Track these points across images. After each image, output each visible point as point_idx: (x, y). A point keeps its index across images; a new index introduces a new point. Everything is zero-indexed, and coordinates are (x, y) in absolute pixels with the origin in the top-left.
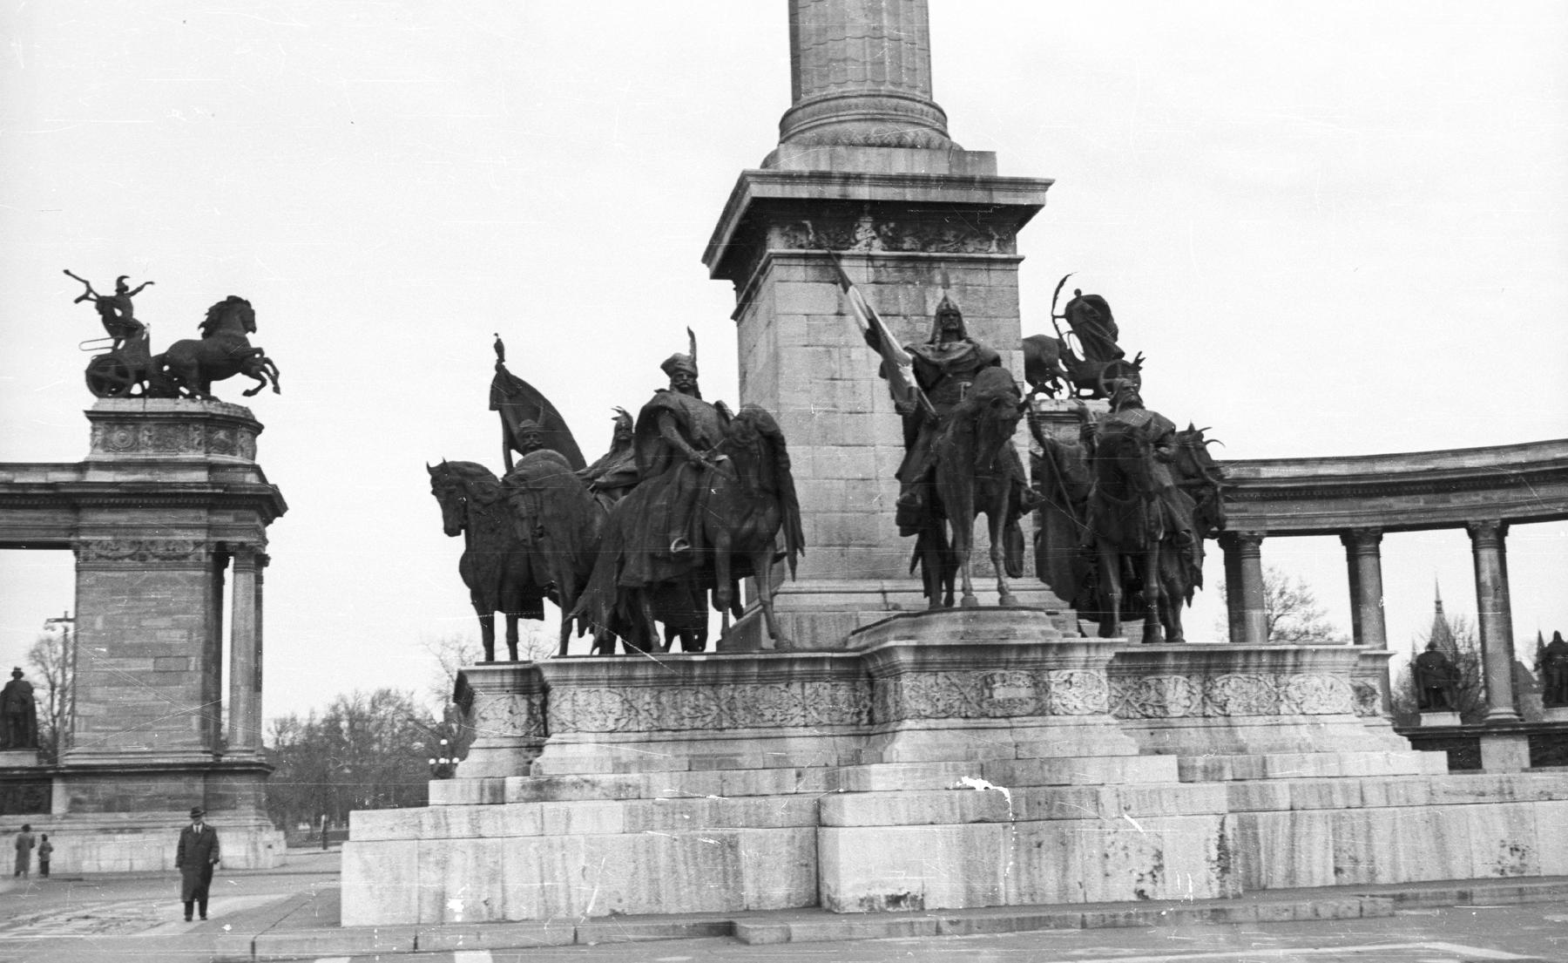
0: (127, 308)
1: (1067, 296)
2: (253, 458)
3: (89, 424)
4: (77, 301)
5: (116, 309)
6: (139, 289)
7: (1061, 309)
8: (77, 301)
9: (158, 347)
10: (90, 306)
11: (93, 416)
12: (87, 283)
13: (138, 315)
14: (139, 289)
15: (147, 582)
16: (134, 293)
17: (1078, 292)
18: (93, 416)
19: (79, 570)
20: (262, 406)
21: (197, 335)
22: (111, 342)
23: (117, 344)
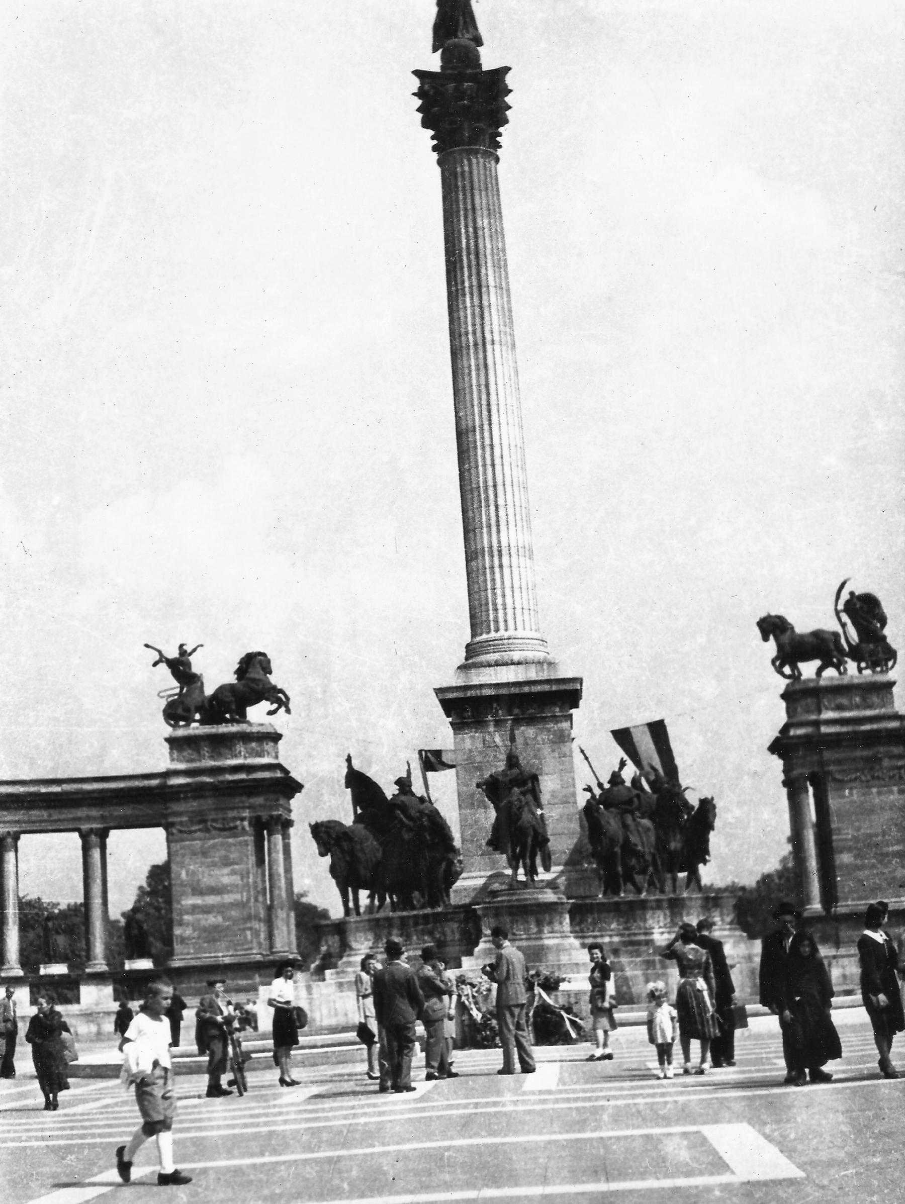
0: (188, 665)
1: (845, 596)
2: (277, 757)
3: (167, 745)
4: (155, 664)
5: (180, 667)
6: (194, 650)
7: (841, 606)
8: (155, 664)
9: (209, 690)
10: (163, 668)
11: (171, 741)
12: (160, 652)
13: (195, 669)
14: (194, 650)
15: (214, 846)
16: (190, 654)
17: (852, 594)
18: (171, 741)
19: (168, 841)
20: (280, 722)
21: (232, 679)
22: (177, 691)
23: (182, 689)
